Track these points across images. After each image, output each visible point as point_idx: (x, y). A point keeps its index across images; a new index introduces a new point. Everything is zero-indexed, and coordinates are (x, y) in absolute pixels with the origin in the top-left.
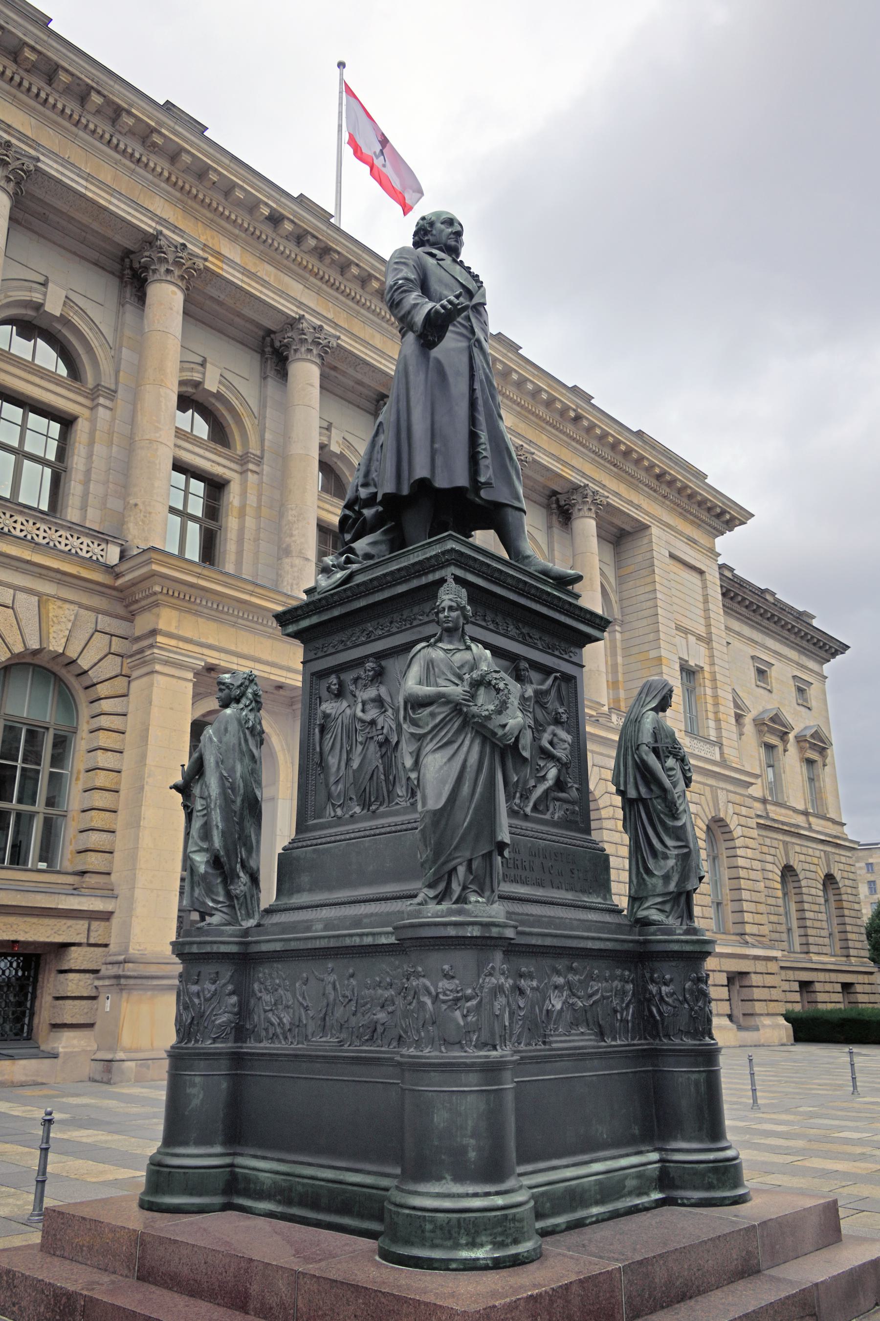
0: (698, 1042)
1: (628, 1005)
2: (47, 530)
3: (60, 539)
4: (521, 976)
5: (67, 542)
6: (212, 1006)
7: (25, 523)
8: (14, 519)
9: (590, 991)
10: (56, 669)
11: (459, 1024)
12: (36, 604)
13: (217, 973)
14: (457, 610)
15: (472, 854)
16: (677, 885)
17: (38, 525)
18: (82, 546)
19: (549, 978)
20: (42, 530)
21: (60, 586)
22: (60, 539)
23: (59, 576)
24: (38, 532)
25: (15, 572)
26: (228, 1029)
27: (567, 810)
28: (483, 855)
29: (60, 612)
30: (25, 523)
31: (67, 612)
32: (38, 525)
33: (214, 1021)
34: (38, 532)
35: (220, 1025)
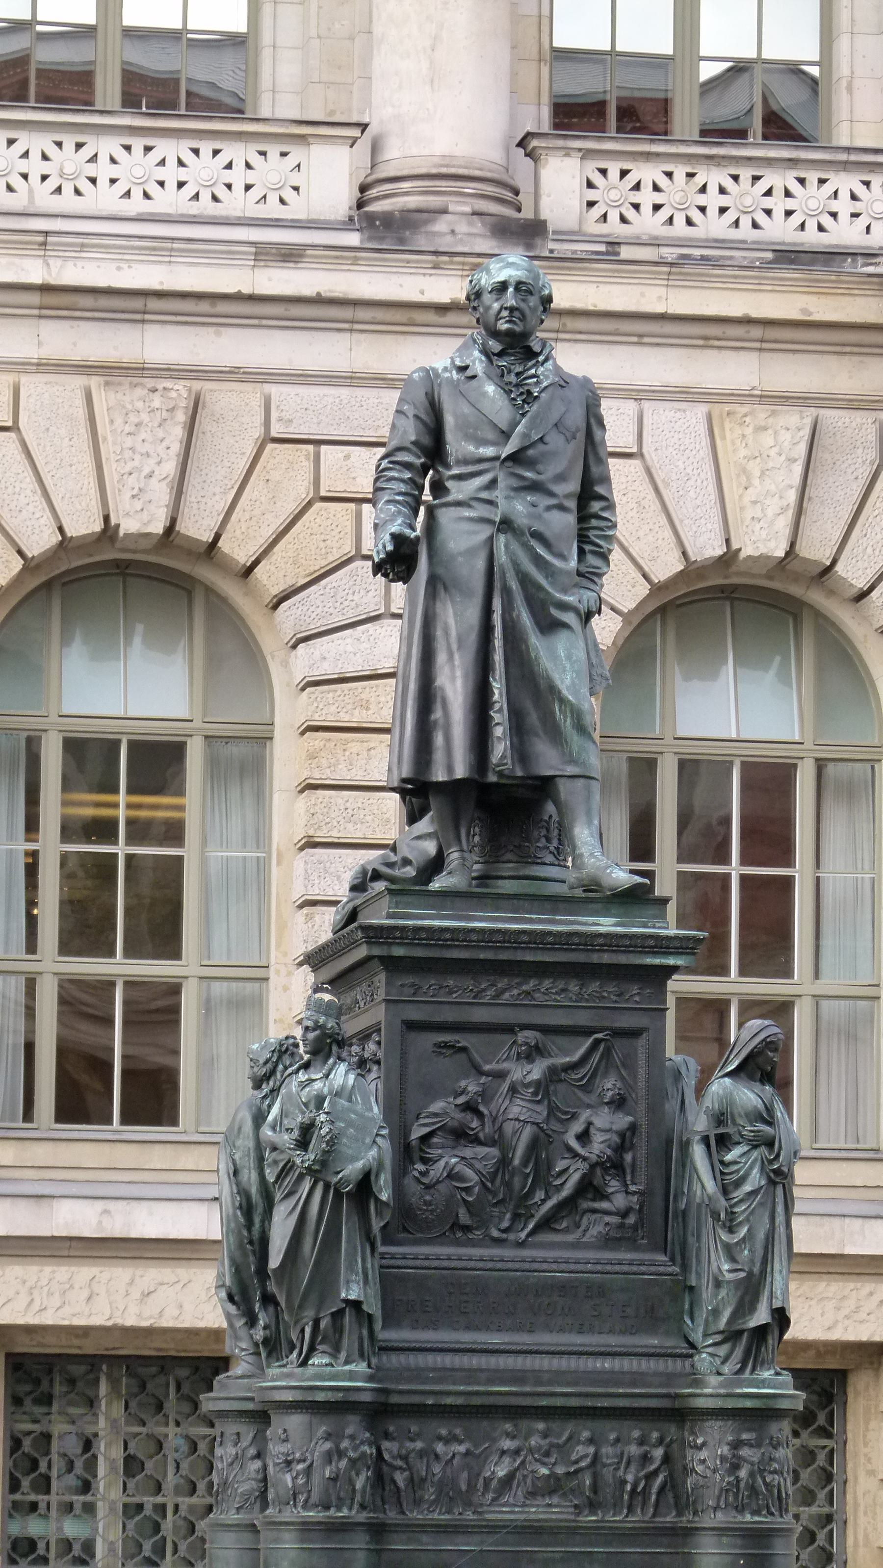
0: (732, 1520)
1: (655, 1473)
2: (729, 184)
3: (768, 203)
4: (440, 1438)
5: (790, 204)
6: (235, 1472)
7: (663, 181)
8: (631, 180)
9: (574, 1457)
10: (795, 590)
11: (287, 1486)
12: (703, 429)
13: (238, 1434)
14: (314, 1030)
15: (318, 1311)
16: (729, 1322)
17: (699, 180)
18: (834, 206)
19: (494, 1440)
20: (713, 189)
21: (766, 355)
22: (768, 203)
23: (756, 332)
24: (702, 200)
25: (637, 349)
26: (252, 1499)
27: (607, 1224)
28: (333, 1314)
29: (767, 439)
30: (663, 181)
31: (786, 437)
32: (699, 180)
33: (236, 1490)
34: (702, 200)
35: (242, 1494)
